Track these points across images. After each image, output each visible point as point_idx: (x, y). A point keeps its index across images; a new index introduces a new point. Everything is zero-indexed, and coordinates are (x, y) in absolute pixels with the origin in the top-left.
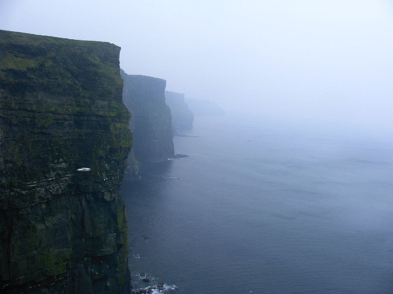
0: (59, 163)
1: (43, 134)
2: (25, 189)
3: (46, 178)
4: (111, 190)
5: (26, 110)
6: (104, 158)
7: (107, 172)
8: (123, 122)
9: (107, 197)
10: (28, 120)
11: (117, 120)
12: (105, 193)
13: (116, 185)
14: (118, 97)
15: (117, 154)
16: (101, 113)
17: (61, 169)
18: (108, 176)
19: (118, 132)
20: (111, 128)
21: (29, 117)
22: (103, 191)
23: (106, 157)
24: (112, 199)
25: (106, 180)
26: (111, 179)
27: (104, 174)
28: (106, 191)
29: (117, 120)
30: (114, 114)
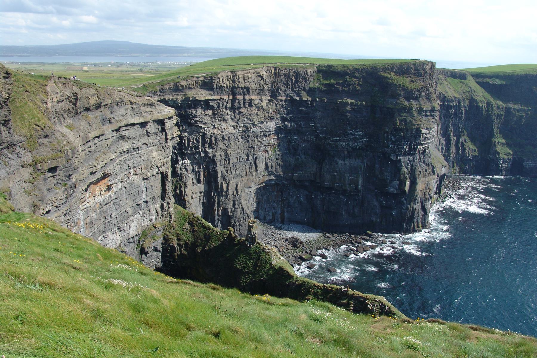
0: (357, 132)
2: (332, 141)
7: (393, 142)
17: (360, 135)
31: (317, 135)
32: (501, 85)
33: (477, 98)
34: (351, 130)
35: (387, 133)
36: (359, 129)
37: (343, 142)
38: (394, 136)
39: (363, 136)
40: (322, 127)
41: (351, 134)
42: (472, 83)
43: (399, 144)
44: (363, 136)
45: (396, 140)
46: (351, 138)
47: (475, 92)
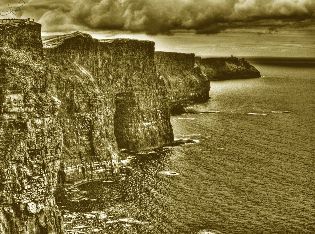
4: (37, 200)
6: (23, 162)
7: (29, 178)
8: (47, 117)
9: (32, 208)
11: (37, 115)
12: (29, 204)
13: (42, 193)
14: (39, 87)
18: (30, 183)
19: (38, 130)
20: (28, 126)
22: (26, 202)
23: (25, 162)
24: (38, 211)
26: (35, 186)
28: (30, 202)
30: (32, 109)
35: (18, 162)
43: (38, 181)
45: (34, 174)
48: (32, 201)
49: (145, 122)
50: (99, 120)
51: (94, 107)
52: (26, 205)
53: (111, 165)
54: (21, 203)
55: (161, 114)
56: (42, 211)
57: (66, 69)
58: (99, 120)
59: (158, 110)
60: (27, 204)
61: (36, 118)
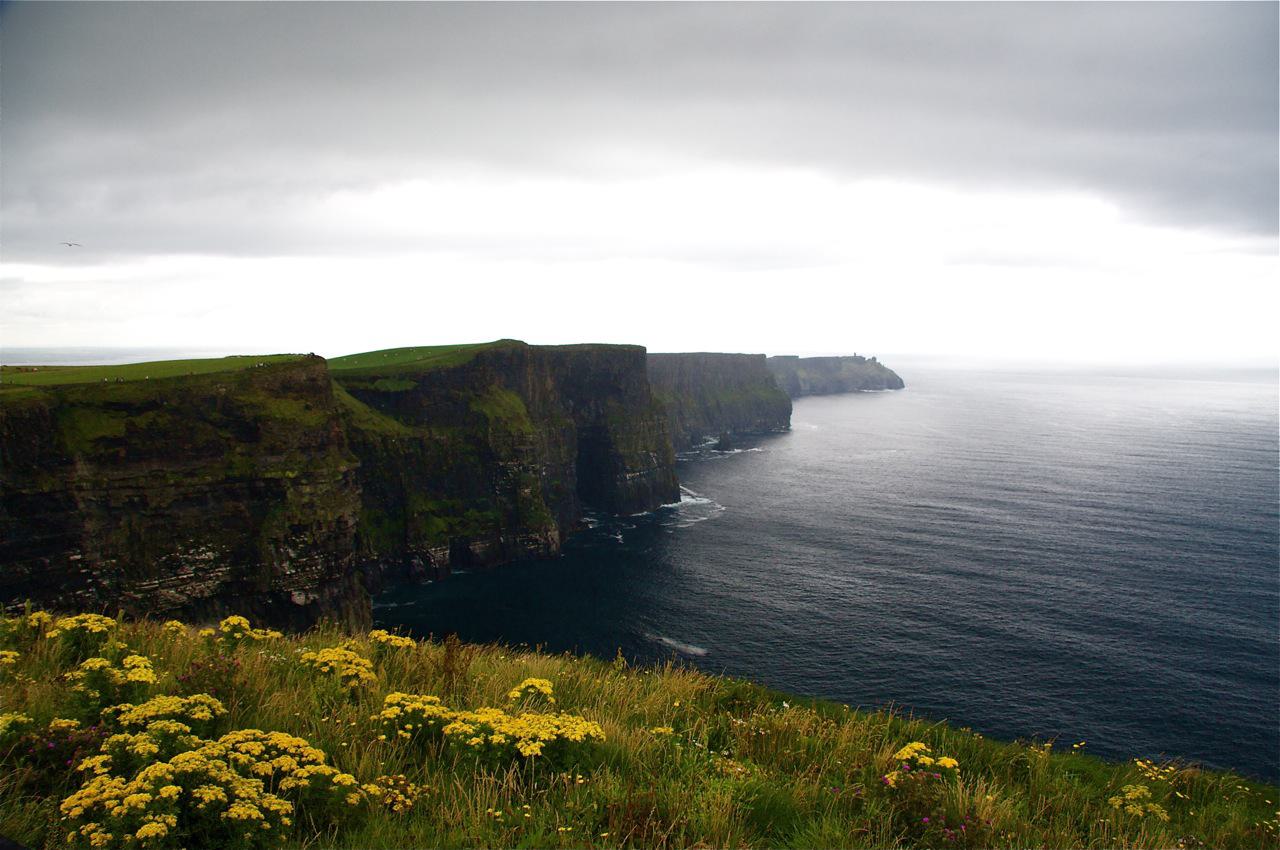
0: (199, 554)
1: (162, 516)
2: (140, 591)
3: (176, 575)
5: (130, 487)
6: (282, 540)
9: (299, 599)
10: (136, 499)
11: (304, 481)
15: (308, 533)
16: (268, 475)
18: (296, 568)
19: (306, 500)
21: (138, 496)
24: (308, 602)
25: (292, 574)
27: (286, 565)
29: (304, 481)
31: (96, 584)
32: (397, 394)
33: (363, 427)
34: (186, 552)
35: (276, 541)
36: (205, 544)
37: (170, 587)
38: (294, 546)
39: (217, 562)
40: (106, 557)
41: (186, 560)
42: (340, 394)
44: (217, 562)
45: (300, 556)
46: (189, 572)
47: (353, 412)
48: (299, 590)
49: (628, 472)
50: (531, 472)
51: (522, 452)
52: (290, 595)
53: (546, 539)
54: (281, 591)
55: (657, 459)
56: (314, 600)
57: (479, 396)
58: (531, 472)
59: (651, 454)
60: (291, 592)
61: (303, 484)
